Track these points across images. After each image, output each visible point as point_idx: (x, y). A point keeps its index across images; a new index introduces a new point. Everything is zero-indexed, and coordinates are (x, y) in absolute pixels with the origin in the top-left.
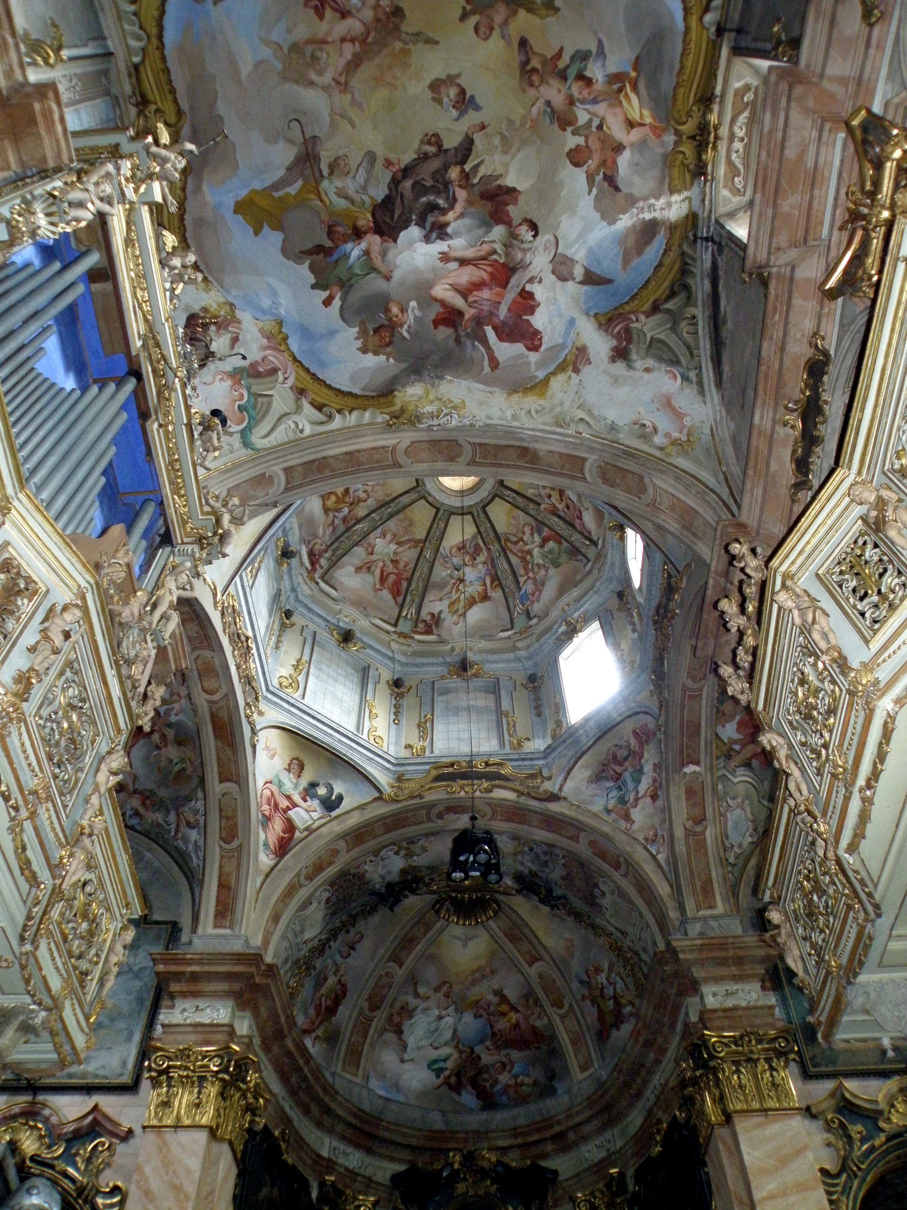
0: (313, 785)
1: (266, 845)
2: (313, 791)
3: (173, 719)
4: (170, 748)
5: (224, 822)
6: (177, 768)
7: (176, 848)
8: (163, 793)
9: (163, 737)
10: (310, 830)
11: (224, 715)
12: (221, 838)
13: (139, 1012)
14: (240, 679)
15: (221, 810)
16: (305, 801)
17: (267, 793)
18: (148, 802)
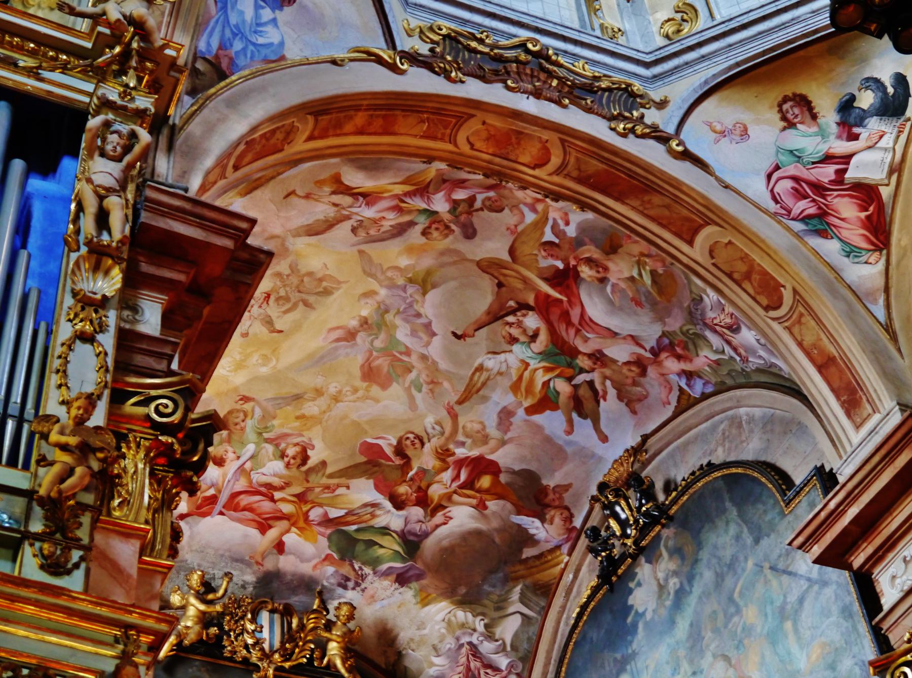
0: (847, 106)
1: (851, 251)
2: (855, 113)
3: (571, 231)
4: (610, 265)
5: (747, 285)
6: (647, 280)
7: (759, 370)
8: (675, 323)
9: (589, 261)
10: (896, 169)
11: (595, 165)
12: (767, 308)
13: (855, 627)
14: (558, 103)
15: (730, 276)
16: (855, 137)
17: (784, 187)
18: (679, 350)
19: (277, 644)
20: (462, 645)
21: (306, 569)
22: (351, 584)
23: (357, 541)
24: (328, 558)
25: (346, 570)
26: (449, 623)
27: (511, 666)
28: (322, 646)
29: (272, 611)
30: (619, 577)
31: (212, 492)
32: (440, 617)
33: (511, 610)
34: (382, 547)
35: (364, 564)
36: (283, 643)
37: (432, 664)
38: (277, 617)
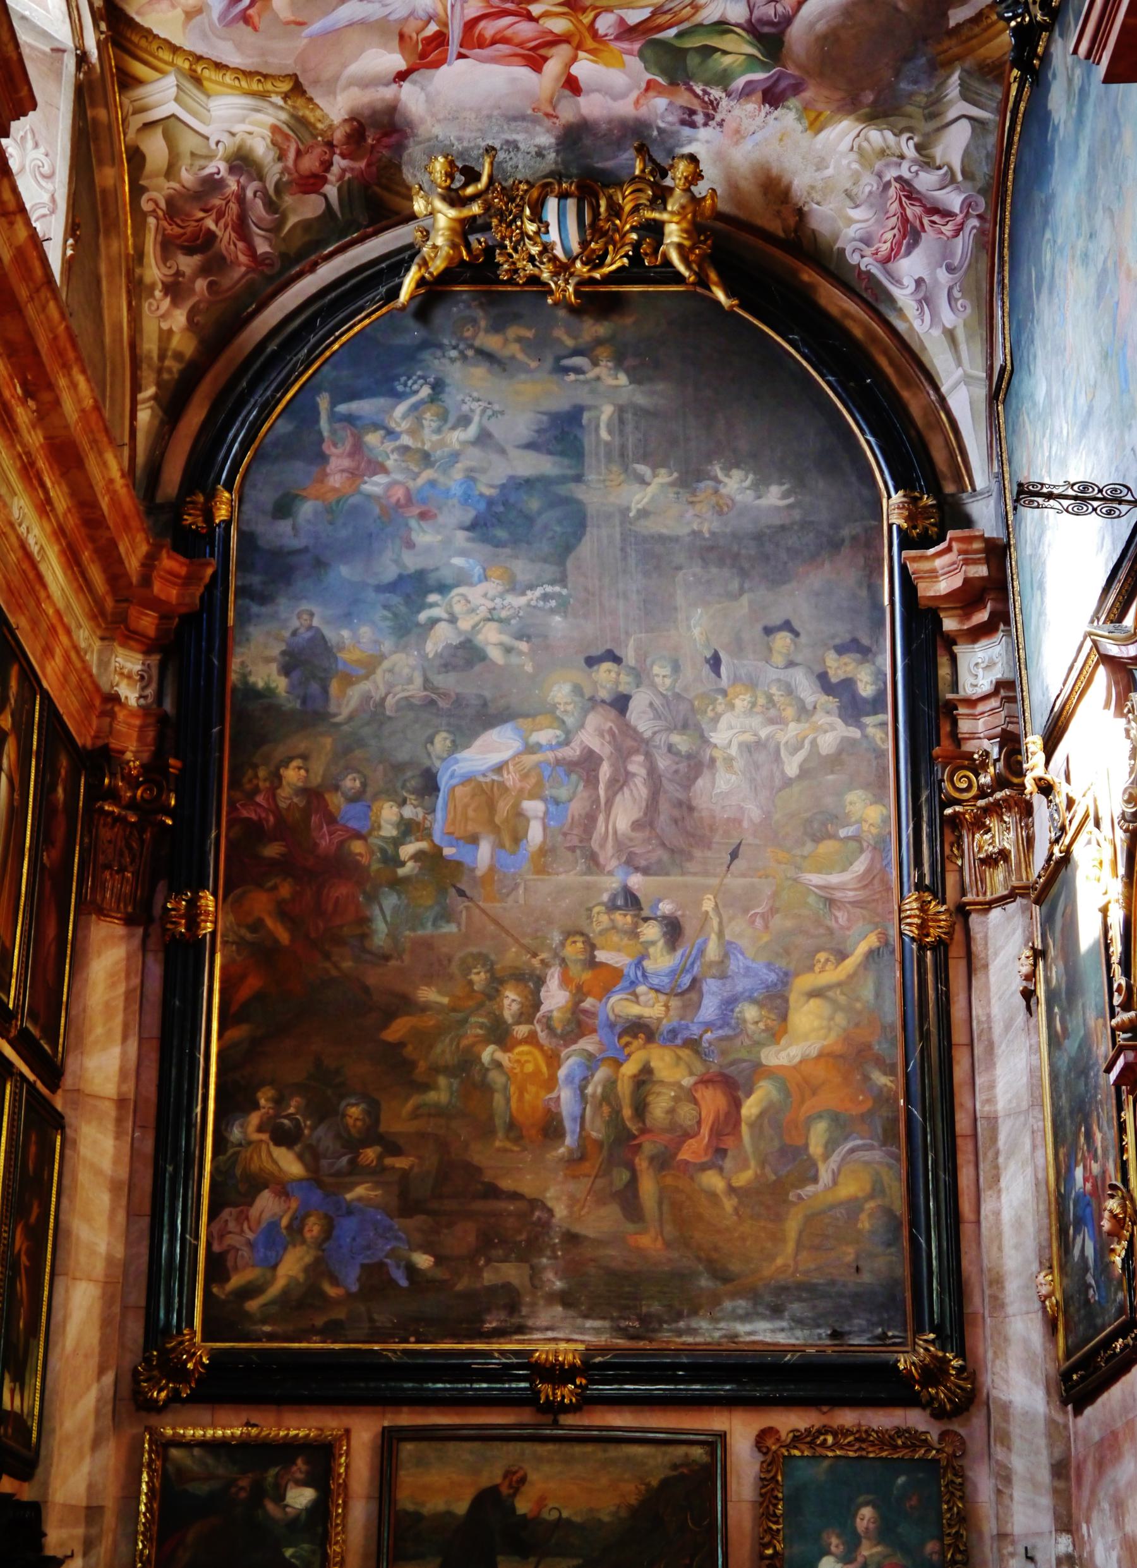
19: (576, 248)
20: (887, 185)
21: (625, 108)
22: (699, 118)
23: (686, 51)
24: (650, 86)
25: (684, 99)
26: (861, 152)
27: (967, 205)
28: (655, 230)
29: (563, 196)
30: (1041, 59)
31: (433, 28)
32: (845, 145)
33: (952, 114)
34: (725, 53)
35: (707, 84)
36: (584, 244)
37: (850, 221)
38: (571, 204)
